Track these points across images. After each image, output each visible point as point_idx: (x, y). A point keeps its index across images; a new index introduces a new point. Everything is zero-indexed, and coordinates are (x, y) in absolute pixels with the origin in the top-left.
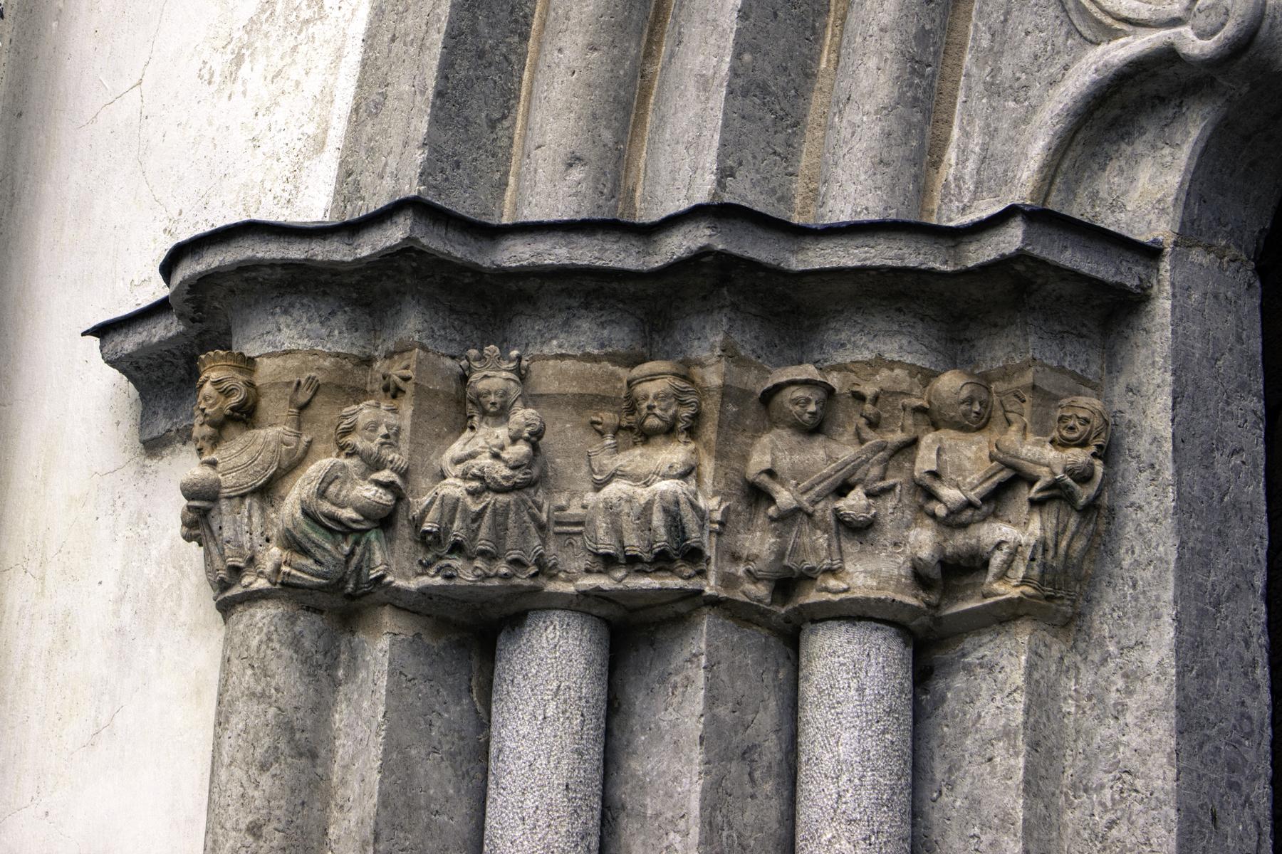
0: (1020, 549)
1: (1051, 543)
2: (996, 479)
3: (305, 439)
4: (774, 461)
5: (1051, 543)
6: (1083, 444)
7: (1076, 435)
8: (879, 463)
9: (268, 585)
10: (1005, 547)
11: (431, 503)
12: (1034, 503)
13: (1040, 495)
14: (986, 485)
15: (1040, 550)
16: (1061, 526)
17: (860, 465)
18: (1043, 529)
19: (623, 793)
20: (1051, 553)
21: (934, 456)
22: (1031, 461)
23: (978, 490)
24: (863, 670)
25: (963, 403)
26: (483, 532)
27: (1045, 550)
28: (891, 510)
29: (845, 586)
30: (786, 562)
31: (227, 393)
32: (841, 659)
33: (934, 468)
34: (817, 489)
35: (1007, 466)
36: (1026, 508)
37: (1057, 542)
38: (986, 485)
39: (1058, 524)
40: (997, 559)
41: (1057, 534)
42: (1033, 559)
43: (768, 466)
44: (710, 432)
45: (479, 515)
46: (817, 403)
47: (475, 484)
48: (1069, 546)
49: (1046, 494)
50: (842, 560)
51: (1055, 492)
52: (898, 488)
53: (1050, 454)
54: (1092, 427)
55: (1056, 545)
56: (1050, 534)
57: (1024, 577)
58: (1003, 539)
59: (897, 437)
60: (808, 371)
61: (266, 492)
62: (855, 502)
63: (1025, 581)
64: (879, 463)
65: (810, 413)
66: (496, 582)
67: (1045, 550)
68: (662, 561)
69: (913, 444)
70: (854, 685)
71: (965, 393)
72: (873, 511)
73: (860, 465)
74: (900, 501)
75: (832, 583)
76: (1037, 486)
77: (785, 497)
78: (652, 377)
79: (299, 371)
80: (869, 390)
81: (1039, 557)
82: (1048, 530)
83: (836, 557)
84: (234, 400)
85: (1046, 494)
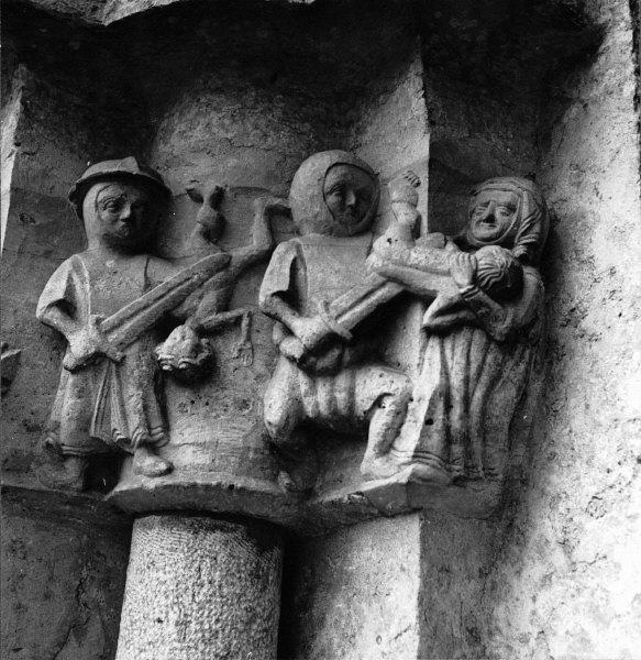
0: (411, 406)
1: (457, 396)
2: (373, 299)
4: (70, 290)
5: (457, 396)
7: (496, 230)
10: (388, 402)
12: (430, 332)
13: (439, 320)
14: (358, 309)
15: (441, 406)
17: (189, 291)
18: (445, 372)
20: (457, 411)
22: (425, 269)
23: (346, 317)
24: (190, 592)
25: (330, 193)
27: (448, 407)
29: (163, 466)
30: (92, 433)
32: (161, 574)
35: (391, 279)
37: (466, 392)
38: (358, 309)
41: (466, 380)
42: (429, 422)
48: (487, 397)
49: (449, 318)
50: (167, 428)
51: (462, 314)
53: (451, 257)
54: (519, 218)
55: (467, 400)
56: (456, 380)
57: (416, 450)
58: (386, 391)
59: (241, 252)
60: (130, 165)
62: (176, 347)
63: (419, 454)
65: (123, 220)
67: (448, 407)
70: (173, 617)
71: (332, 179)
72: (202, 356)
73: (189, 291)
74: (249, 339)
76: (434, 307)
81: (439, 416)
83: (157, 423)
85: (449, 318)
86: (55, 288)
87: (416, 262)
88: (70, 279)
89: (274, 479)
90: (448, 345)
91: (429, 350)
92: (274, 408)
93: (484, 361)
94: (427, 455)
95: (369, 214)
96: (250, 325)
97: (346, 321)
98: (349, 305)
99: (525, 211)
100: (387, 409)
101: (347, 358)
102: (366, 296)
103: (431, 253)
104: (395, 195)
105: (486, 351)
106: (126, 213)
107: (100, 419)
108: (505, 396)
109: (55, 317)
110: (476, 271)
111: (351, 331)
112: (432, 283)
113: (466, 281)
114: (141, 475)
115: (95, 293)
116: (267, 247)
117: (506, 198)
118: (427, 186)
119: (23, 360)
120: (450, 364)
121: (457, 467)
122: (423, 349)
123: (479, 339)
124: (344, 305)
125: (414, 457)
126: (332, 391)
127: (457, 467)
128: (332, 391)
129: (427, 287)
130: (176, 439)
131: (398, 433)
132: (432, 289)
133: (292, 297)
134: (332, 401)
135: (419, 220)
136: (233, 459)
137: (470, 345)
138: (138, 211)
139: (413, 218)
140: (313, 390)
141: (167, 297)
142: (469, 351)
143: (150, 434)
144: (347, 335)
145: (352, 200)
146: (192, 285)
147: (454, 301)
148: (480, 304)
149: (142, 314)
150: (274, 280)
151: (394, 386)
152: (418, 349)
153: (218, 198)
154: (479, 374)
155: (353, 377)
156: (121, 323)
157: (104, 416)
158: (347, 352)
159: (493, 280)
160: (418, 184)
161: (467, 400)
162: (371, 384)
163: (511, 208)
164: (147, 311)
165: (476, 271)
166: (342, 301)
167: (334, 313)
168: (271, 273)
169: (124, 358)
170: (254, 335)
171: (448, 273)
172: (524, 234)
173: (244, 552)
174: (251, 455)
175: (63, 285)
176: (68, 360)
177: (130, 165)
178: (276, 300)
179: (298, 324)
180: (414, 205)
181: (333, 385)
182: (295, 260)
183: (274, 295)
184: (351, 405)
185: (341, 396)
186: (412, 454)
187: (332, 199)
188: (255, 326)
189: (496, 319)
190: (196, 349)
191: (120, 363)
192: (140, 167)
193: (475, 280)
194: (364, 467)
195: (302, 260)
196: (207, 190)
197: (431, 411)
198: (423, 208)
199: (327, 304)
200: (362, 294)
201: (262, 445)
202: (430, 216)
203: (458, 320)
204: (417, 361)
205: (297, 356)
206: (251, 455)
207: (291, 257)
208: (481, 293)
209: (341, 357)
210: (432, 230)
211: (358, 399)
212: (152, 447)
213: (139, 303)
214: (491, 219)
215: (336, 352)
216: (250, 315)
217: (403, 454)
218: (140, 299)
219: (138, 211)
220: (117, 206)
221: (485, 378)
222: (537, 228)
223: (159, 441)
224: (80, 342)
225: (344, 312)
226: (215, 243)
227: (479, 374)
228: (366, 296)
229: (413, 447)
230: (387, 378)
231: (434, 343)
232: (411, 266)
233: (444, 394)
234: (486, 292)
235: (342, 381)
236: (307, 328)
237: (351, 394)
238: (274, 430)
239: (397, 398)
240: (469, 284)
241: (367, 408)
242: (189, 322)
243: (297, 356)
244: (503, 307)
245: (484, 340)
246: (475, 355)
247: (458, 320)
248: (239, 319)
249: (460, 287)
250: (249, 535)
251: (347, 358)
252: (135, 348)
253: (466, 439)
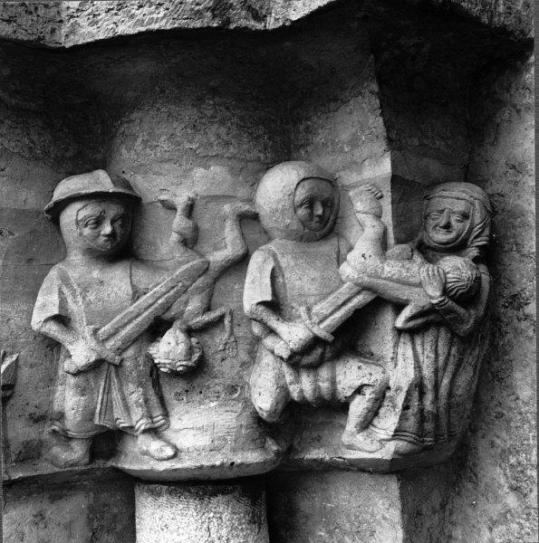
1: (429, 385)
2: (350, 305)
5: (429, 385)
6: (457, 248)
8: (200, 290)
12: (400, 332)
13: (411, 324)
14: (338, 315)
15: (416, 394)
16: (441, 359)
17: (175, 297)
18: (418, 367)
20: (429, 397)
21: (268, 281)
22: (398, 281)
23: (327, 322)
25: (301, 206)
27: (422, 394)
28: (221, 347)
29: (170, 452)
30: (97, 422)
33: (268, 298)
34: (123, 333)
35: (364, 288)
36: (389, 338)
39: (437, 355)
40: (358, 407)
41: (436, 372)
42: (406, 407)
43: (56, 311)
46: (113, 222)
48: (452, 382)
49: (419, 321)
50: (166, 415)
51: (431, 317)
52: (227, 321)
53: (418, 269)
55: (436, 387)
56: (427, 372)
57: (396, 431)
58: (366, 382)
59: (218, 257)
60: (101, 181)
62: (170, 349)
63: (398, 434)
64: (200, 290)
69: (241, 263)
71: (301, 194)
72: (196, 356)
74: (232, 333)
76: (406, 313)
82: (424, 366)
83: (157, 412)
85: (419, 321)
86: (47, 303)
87: (390, 275)
88: (61, 293)
89: (263, 447)
90: (418, 341)
91: (401, 345)
92: (264, 401)
93: (449, 354)
94: (405, 434)
95: (332, 218)
96: (231, 322)
97: (329, 326)
98: (329, 311)
99: (478, 218)
100: (368, 396)
101: (328, 355)
102: (344, 304)
103: (403, 266)
104: (359, 206)
105: (451, 344)
106: (107, 229)
107: (103, 411)
108: (464, 378)
109: (53, 330)
110: (446, 283)
111: (333, 334)
112: (402, 293)
113: (438, 294)
114: (145, 455)
115: (88, 304)
116: (241, 252)
117: (460, 207)
118: (390, 200)
119: (21, 363)
120: (421, 358)
121: (429, 439)
122: (396, 345)
123: (444, 335)
124: (326, 312)
125: (393, 436)
126: (316, 381)
127: (429, 439)
128: (316, 381)
129: (400, 296)
130: (175, 423)
131: (376, 414)
132: (405, 298)
133: (275, 306)
134: (317, 389)
135: (385, 233)
136: (229, 438)
137: (437, 342)
138: (116, 225)
139: (379, 229)
140: (297, 380)
141: (156, 305)
142: (437, 346)
143: (153, 423)
144: (330, 338)
145: (319, 211)
146: (177, 292)
147: (425, 309)
148: (450, 311)
149: (135, 322)
150: (254, 289)
151: (373, 379)
152: (392, 345)
153: (190, 210)
154: (445, 369)
155: (334, 368)
156: (116, 332)
157: (108, 407)
158: (328, 350)
159: (460, 292)
160: (381, 197)
161: (436, 387)
162: (349, 375)
163: (465, 216)
164: (139, 319)
165: (446, 283)
166: (322, 308)
167: (316, 319)
168: (253, 282)
169: (122, 360)
170: (236, 330)
171: (420, 285)
172: (476, 237)
173: (242, 507)
174: (243, 431)
175: (55, 298)
176: (67, 365)
177: (101, 181)
178: (261, 308)
179: (281, 327)
180: (378, 216)
181: (316, 375)
182: (273, 270)
183: (259, 303)
184: (334, 391)
185: (324, 385)
186: (392, 433)
187: (302, 212)
188: (235, 322)
189: (462, 322)
190: (190, 351)
191: (119, 367)
192: (113, 182)
193: (445, 292)
194: (345, 438)
195: (280, 268)
196: (181, 200)
197: (407, 400)
198: (388, 218)
199: (309, 310)
200: (340, 302)
201: (251, 421)
202: (395, 227)
203: (427, 322)
204: (391, 355)
205: (285, 356)
206: (243, 431)
207: (269, 268)
208: (450, 302)
209: (323, 354)
210: (399, 241)
211: (339, 387)
212: (154, 432)
213: (131, 312)
214: (448, 227)
215: (319, 351)
216: (231, 313)
217: (383, 432)
218: (131, 309)
219: (116, 225)
220: (98, 222)
221: (451, 368)
222: (487, 232)
223: (161, 426)
224: (80, 352)
225: (326, 318)
226: (192, 248)
227: (446, 363)
228: (344, 304)
229: (393, 428)
230: (366, 369)
231: (405, 339)
232: (385, 279)
233: (418, 386)
234: (454, 300)
235: (324, 373)
236: (293, 334)
237: (333, 382)
238: (265, 414)
239: (377, 388)
240: (441, 296)
241: (349, 394)
242: (177, 324)
243: (285, 356)
244: (466, 309)
245: (449, 335)
246: (442, 349)
247: (427, 322)
248: (221, 318)
249: (431, 298)
250: (244, 493)
251: (328, 355)
252: (130, 352)
253: (436, 417)
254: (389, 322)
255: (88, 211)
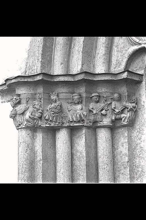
3: (28, 106)
9: (25, 127)
11: (47, 115)
18: (129, 115)
19: (74, 152)
26: (54, 119)
31: (17, 100)
40: (123, 119)
44: (84, 103)
45: (54, 117)
47: (53, 112)
51: (131, 110)
53: (130, 104)
56: (130, 115)
59: (109, 102)
61: (23, 114)
62: (103, 112)
64: (107, 106)
66: (56, 125)
68: (79, 122)
69: (111, 103)
70: (105, 137)
75: (101, 123)
76: (129, 109)
77: (95, 112)
78: (76, 96)
79: (27, 96)
80: (105, 96)
84: (18, 101)
114: (101, 124)
157: (96, 118)
162: (123, 115)
166: (120, 108)
187: (118, 98)
196: (105, 96)
203: (131, 110)
230: (124, 115)
235: (120, 115)
254: (126, 110)
255: (96, 97)
